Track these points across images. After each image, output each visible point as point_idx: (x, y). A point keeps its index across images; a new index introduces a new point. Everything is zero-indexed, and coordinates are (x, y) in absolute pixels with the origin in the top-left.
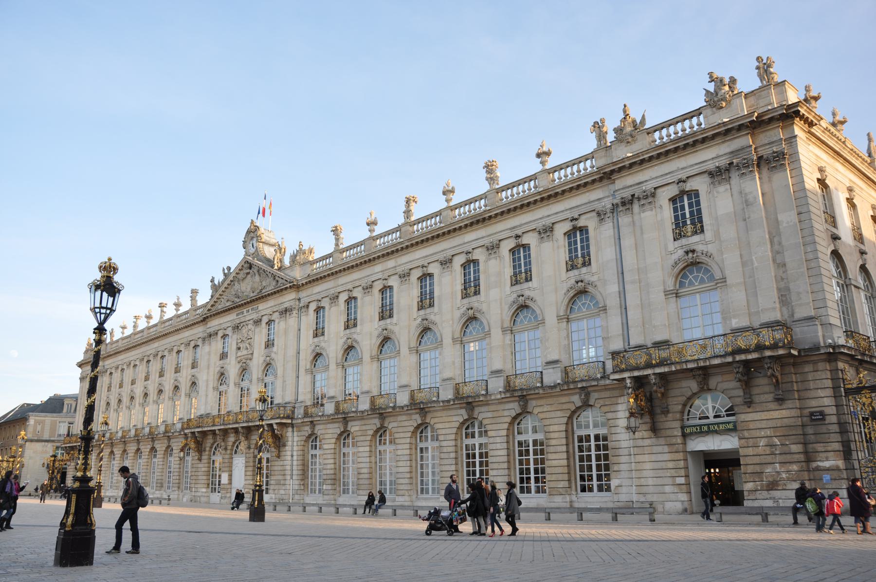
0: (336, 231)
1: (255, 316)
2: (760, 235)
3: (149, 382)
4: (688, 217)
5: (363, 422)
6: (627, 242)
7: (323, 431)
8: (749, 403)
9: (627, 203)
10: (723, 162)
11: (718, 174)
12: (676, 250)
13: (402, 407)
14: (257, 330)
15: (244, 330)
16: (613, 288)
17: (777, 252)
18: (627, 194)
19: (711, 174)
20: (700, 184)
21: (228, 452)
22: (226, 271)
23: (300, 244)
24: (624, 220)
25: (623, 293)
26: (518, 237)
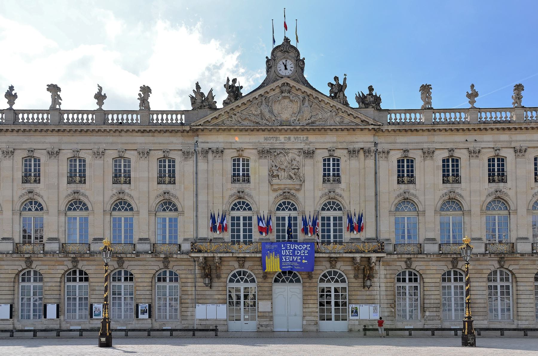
0: (426, 89)
1: (306, 148)
5: (477, 263)
7: (424, 268)
13: (522, 255)
14: (308, 161)
15: (284, 160)
21: (269, 280)
22: (231, 83)
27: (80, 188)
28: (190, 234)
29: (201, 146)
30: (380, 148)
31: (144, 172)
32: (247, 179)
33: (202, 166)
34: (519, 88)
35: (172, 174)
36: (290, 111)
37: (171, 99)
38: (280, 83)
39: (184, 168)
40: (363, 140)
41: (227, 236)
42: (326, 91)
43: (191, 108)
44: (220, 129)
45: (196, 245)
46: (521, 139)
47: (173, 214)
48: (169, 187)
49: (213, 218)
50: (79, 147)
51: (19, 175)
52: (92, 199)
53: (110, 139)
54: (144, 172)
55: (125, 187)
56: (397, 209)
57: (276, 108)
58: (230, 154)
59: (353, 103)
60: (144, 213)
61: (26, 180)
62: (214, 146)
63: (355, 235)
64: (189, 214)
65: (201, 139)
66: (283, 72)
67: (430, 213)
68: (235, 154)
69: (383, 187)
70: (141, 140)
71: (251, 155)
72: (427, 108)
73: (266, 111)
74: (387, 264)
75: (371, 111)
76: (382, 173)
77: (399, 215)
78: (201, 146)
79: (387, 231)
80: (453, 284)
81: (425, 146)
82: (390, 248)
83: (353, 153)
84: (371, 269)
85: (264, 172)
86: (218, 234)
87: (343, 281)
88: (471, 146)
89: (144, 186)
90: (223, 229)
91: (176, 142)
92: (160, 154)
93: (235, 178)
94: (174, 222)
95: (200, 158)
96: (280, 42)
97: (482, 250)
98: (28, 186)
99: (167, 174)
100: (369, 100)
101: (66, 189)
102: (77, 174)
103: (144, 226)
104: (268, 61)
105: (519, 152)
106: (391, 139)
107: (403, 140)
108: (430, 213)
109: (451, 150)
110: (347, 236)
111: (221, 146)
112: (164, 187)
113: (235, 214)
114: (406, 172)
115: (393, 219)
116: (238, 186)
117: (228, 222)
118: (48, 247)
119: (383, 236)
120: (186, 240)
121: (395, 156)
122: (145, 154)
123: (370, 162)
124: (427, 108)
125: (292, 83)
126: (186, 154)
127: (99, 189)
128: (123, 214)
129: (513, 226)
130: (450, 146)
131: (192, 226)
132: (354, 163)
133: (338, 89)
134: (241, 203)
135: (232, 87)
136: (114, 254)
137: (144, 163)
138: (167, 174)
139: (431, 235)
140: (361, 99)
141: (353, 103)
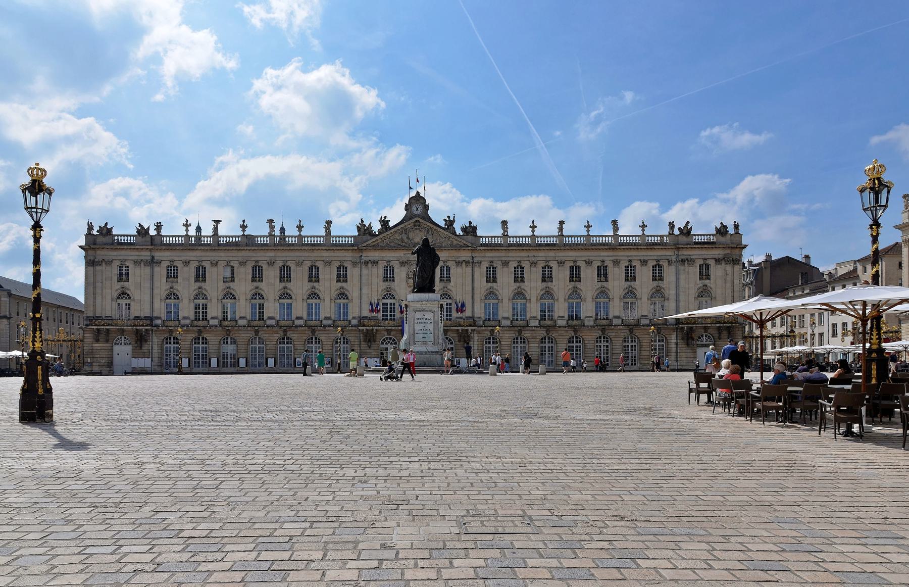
2: (729, 285)
3: (263, 285)
4: (704, 274)
6: (682, 277)
8: (720, 338)
9: (683, 261)
10: (721, 257)
11: (718, 261)
12: (700, 283)
16: (673, 292)
17: (733, 291)
18: (684, 257)
19: (716, 260)
20: (712, 263)
23: (470, 222)
24: (681, 267)
25: (677, 295)
26: (631, 261)
27: (288, 285)
28: (357, 314)
29: (364, 259)
30: (476, 260)
31: (328, 275)
32: (392, 280)
33: (365, 271)
34: (562, 223)
35: (345, 276)
36: (420, 237)
37: (345, 227)
38: (413, 220)
39: (353, 273)
40: (465, 255)
41: (380, 315)
42: (442, 224)
43: (357, 234)
44: (375, 247)
45: (362, 321)
46: (561, 255)
47: (345, 301)
48: (344, 284)
49: (371, 304)
50: (288, 259)
51: (250, 277)
52: (295, 292)
53: (306, 254)
54: (328, 275)
55: (316, 284)
56: (486, 299)
57: (411, 235)
58: (382, 264)
59: (459, 231)
60: (328, 300)
61: (254, 280)
62: (372, 259)
63: (459, 315)
64: (356, 301)
65: (364, 254)
66: (416, 212)
67: (506, 301)
68: (385, 264)
69: (477, 285)
70: (325, 254)
71: (396, 264)
72: (505, 236)
73: (405, 237)
74: (479, 332)
75: (470, 237)
76: (477, 276)
77: (487, 302)
78: (364, 259)
79: (480, 312)
80: (519, 345)
81: (503, 259)
82: (481, 323)
83: (458, 263)
84: (469, 336)
85: (404, 275)
86: (374, 314)
87: (452, 343)
88: (532, 259)
89: (328, 285)
90: (378, 311)
91: (348, 256)
92: (338, 264)
93: (385, 279)
94: (346, 306)
95: (363, 267)
96: (413, 194)
97: (537, 324)
98: (255, 284)
99: (342, 277)
100: (470, 230)
101: (279, 286)
102: (285, 277)
103: (328, 309)
104: (406, 205)
105: (561, 263)
106: (483, 254)
107: (490, 255)
108: (506, 301)
109: (519, 262)
110: (454, 314)
111: (377, 259)
112: (340, 284)
113: (385, 301)
114: (491, 277)
115: (483, 305)
116: (386, 283)
117: (380, 307)
118: (268, 323)
119: (477, 315)
120: (354, 318)
121: (485, 265)
122: (328, 263)
123: (469, 270)
124: (505, 236)
125: (421, 221)
126: (354, 264)
127: (299, 286)
128: (314, 302)
129: (556, 309)
130: (519, 259)
131: (357, 309)
132: (459, 270)
133: (450, 223)
134: (389, 294)
135: (384, 221)
136: (309, 327)
137: (328, 269)
138: (342, 277)
139: (506, 315)
140: (464, 229)
141: (459, 231)
